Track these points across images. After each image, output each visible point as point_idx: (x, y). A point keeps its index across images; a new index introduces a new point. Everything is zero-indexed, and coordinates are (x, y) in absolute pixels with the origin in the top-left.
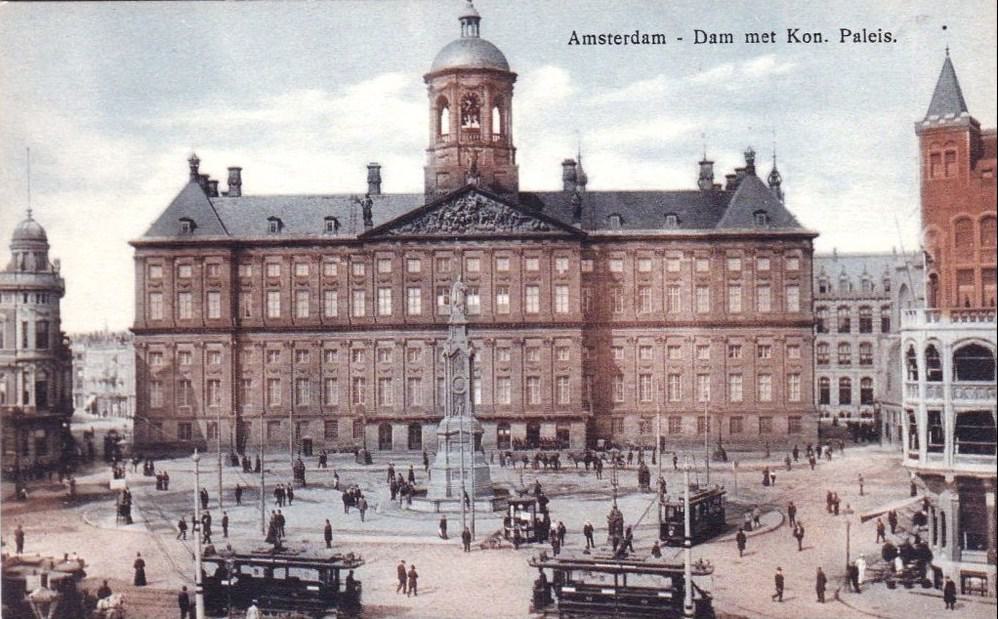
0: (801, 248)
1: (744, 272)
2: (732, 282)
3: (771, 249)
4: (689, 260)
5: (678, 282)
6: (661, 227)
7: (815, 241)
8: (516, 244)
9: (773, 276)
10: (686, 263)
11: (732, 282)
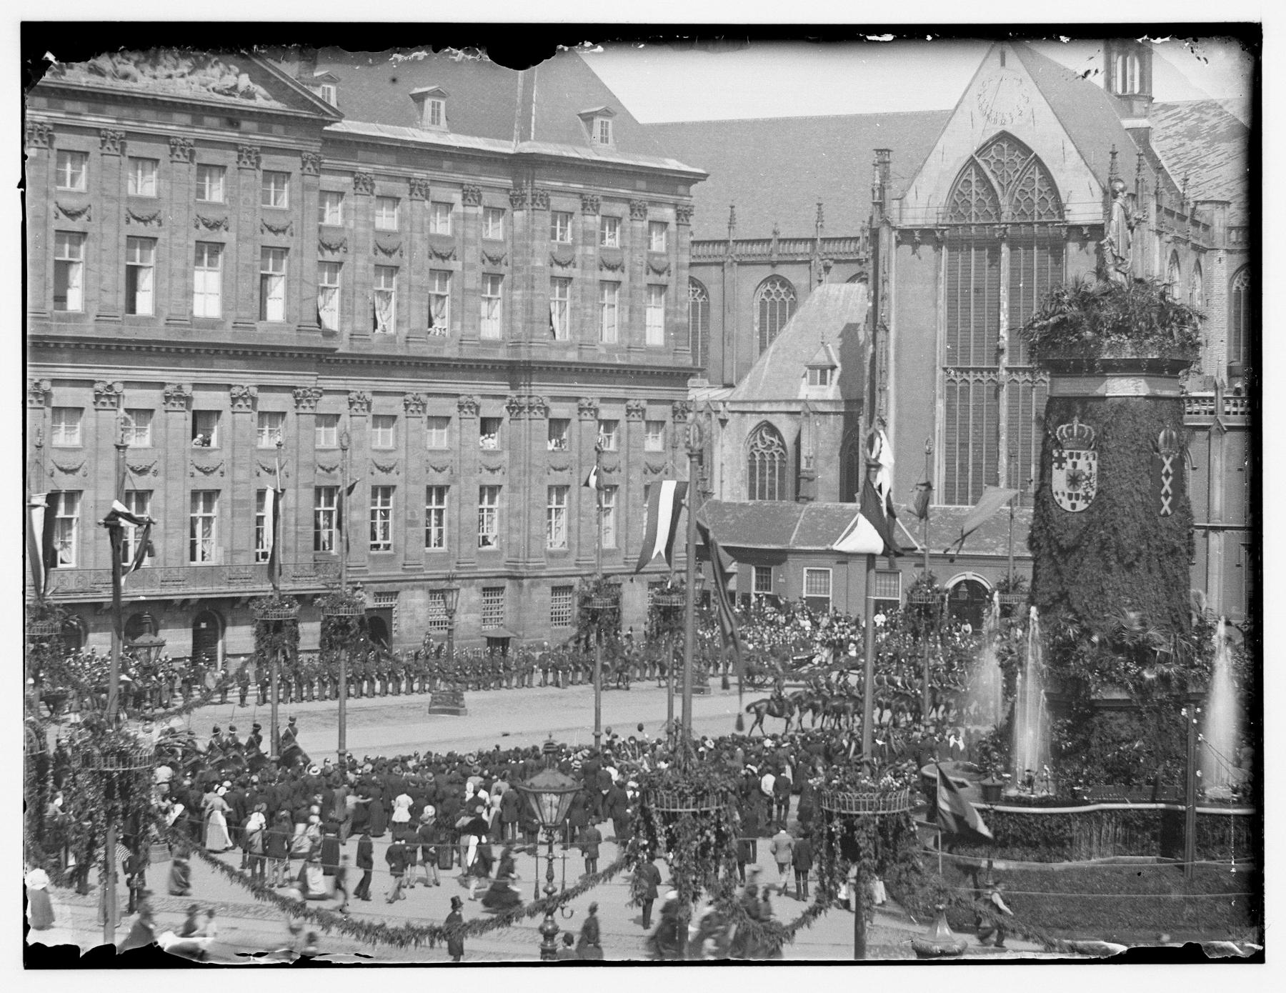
0: (676, 205)
1: (579, 251)
2: (558, 271)
3: (628, 201)
4: (471, 210)
5: (455, 265)
6: (410, 122)
7: (693, 188)
8: (176, 127)
9: (627, 263)
10: (465, 217)
11: (558, 271)
